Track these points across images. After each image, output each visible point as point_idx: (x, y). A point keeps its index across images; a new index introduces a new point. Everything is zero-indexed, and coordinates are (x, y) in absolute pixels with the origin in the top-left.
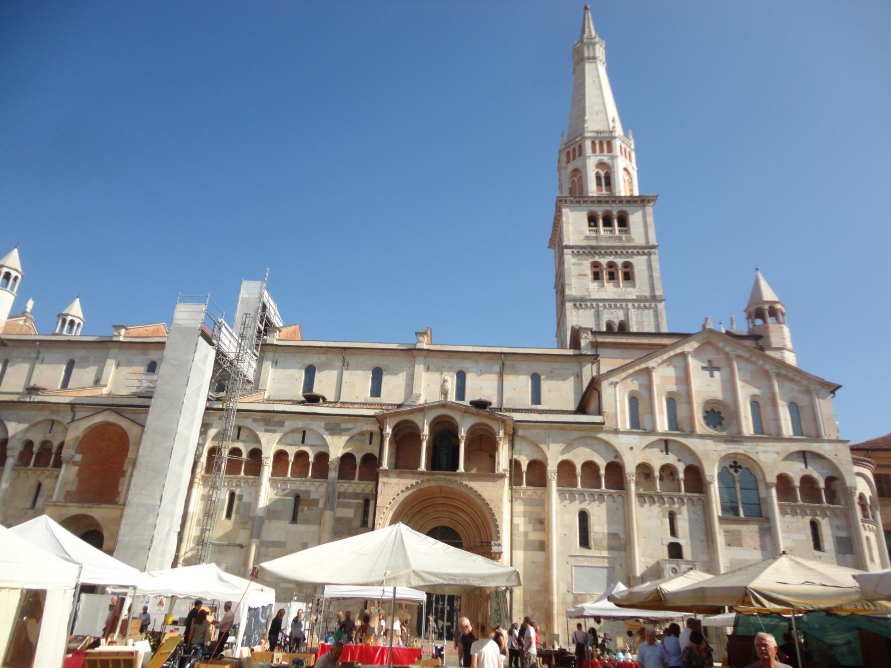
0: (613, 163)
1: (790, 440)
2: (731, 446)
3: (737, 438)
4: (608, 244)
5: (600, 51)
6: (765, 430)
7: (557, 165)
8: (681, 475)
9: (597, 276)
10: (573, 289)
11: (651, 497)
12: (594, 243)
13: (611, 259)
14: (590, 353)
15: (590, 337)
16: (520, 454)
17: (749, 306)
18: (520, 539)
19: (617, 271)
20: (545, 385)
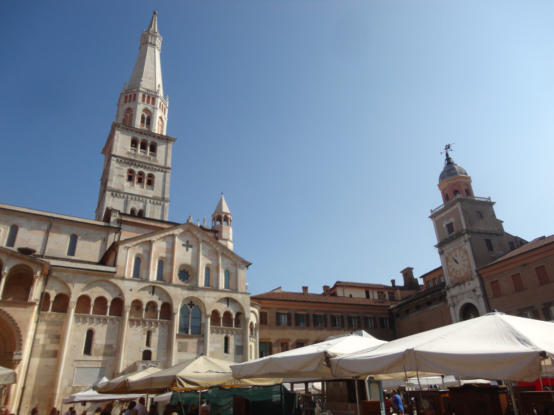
0: (154, 111)
1: (222, 291)
2: (191, 292)
3: (195, 288)
4: (141, 160)
5: (158, 42)
6: (210, 284)
7: (117, 102)
8: (159, 309)
9: (130, 179)
10: (114, 183)
11: (138, 321)
12: (132, 157)
14: (116, 226)
15: (118, 216)
16: (51, 289)
17: (214, 214)
18: (38, 349)
19: (144, 178)
20: (80, 244)
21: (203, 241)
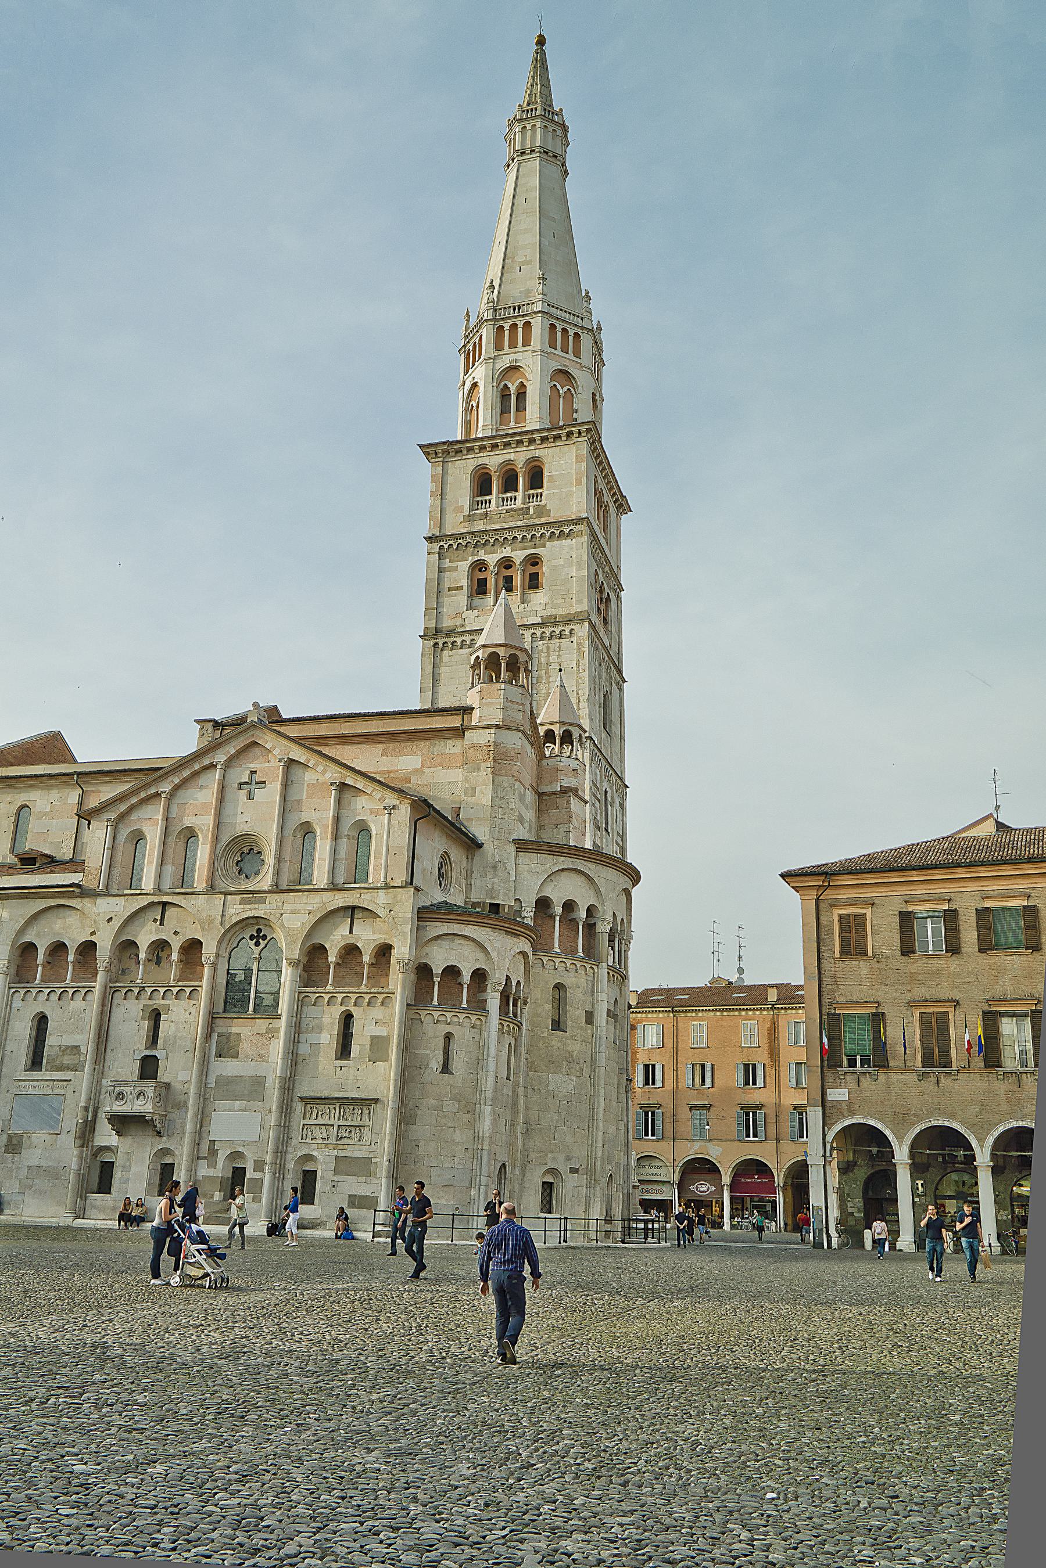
2: (249, 906)
4: (504, 525)
9: (480, 588)
12: (480, 526)
13: (506, 552)
21: (291, 761)
